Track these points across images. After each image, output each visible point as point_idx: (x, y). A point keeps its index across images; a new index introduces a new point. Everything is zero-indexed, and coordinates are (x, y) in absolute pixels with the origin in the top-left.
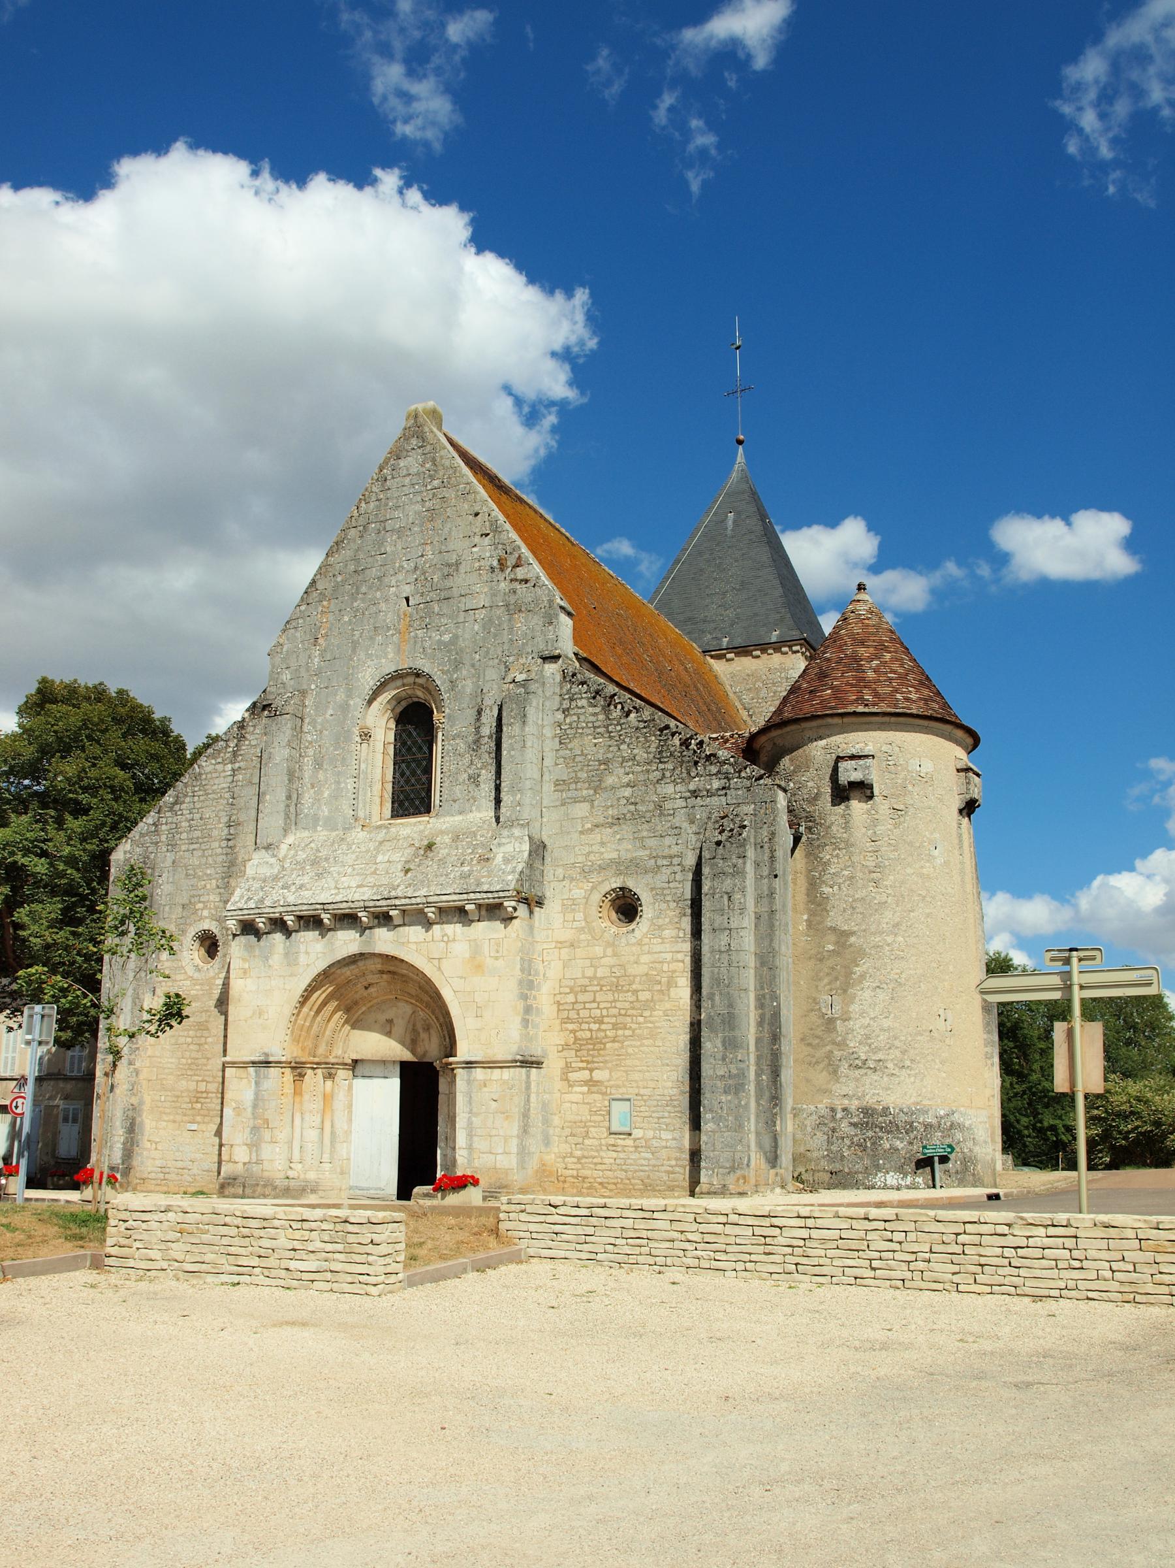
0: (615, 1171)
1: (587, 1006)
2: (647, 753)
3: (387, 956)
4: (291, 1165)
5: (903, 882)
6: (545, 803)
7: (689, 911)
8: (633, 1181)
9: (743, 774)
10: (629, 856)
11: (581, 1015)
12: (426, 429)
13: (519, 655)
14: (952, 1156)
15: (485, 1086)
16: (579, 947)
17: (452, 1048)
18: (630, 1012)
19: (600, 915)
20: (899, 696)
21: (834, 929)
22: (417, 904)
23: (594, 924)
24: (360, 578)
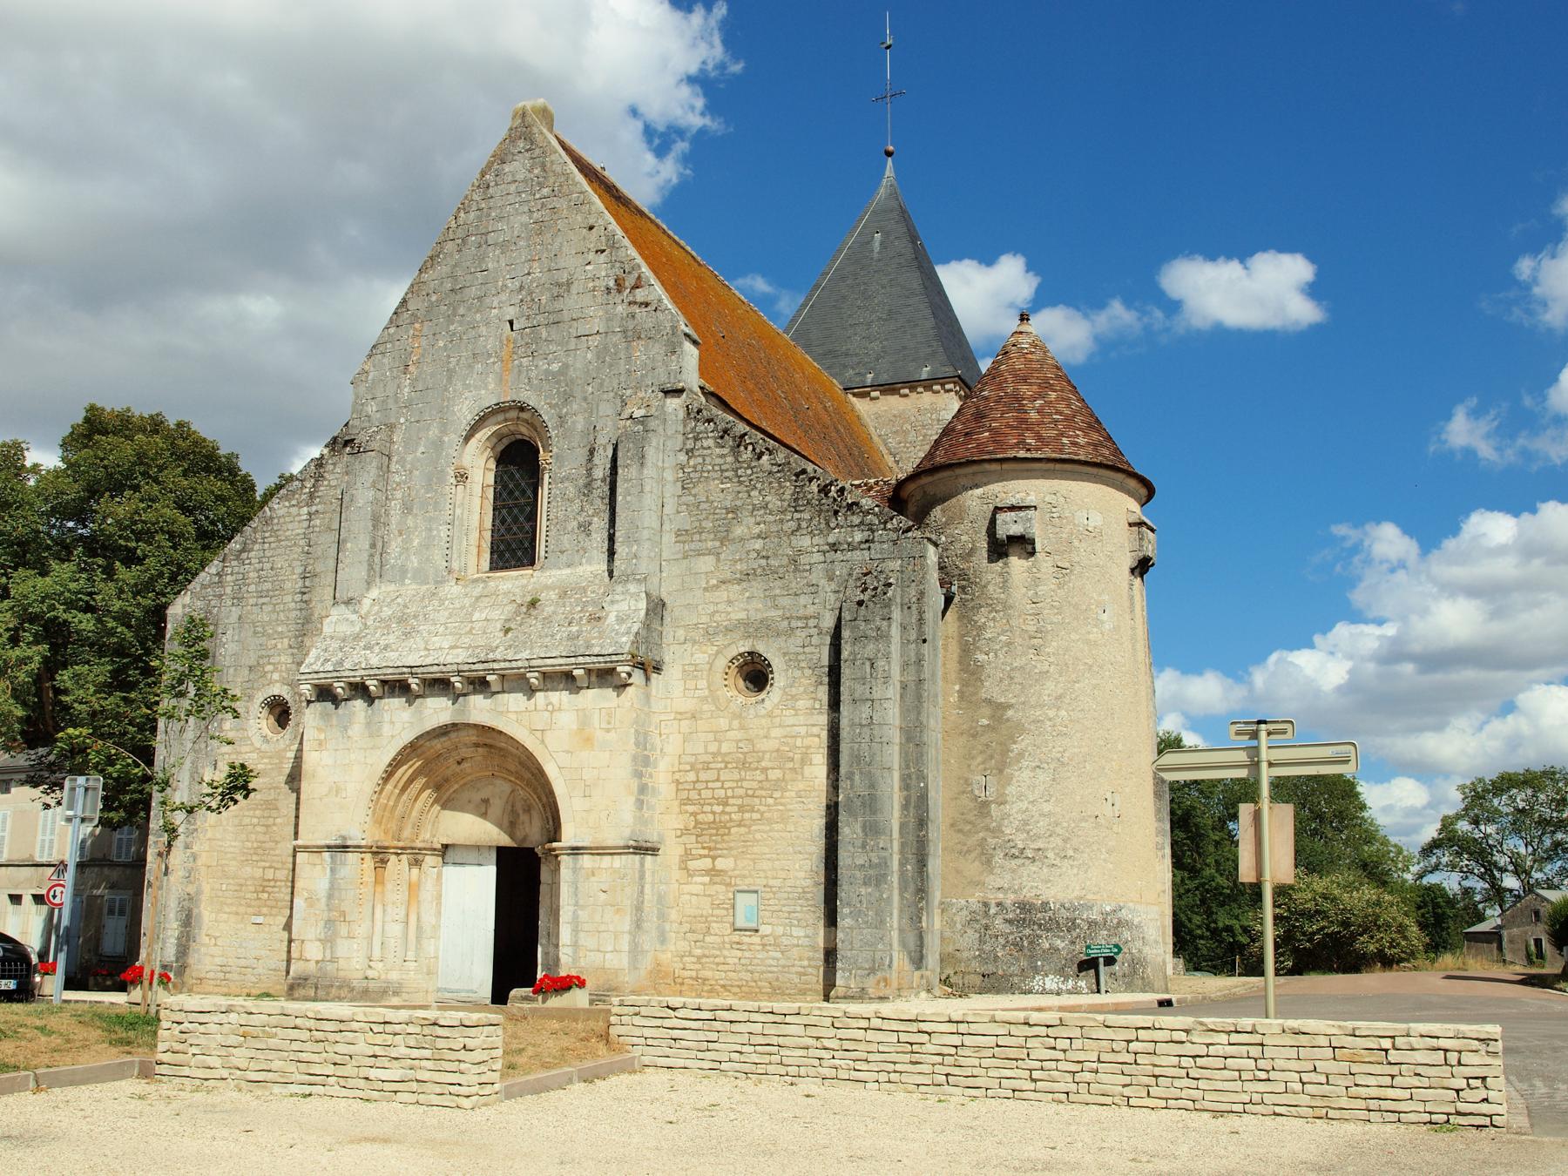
0: (739, 971)
1: (710, 785)
2: (781, 500)
3: (483, 727)
4: (371, 963)
5: (1067, 650)
6: (665, 556)
7: (826, 680)
8: (759, 983)
9: (889, 526)
10: (759, 616)
11: (703, 796)
12: (535, 130)
13: (637, 388)
14: (1119, 958)
15: (593, 875)
16: (702, 719)
17: (555, 833)
18: (758, 793)
19: (726, 683)
20: (1065, 440)
21: (989, 702)
22: (519, 668)
23: (718, 693)
24: (458, 297)
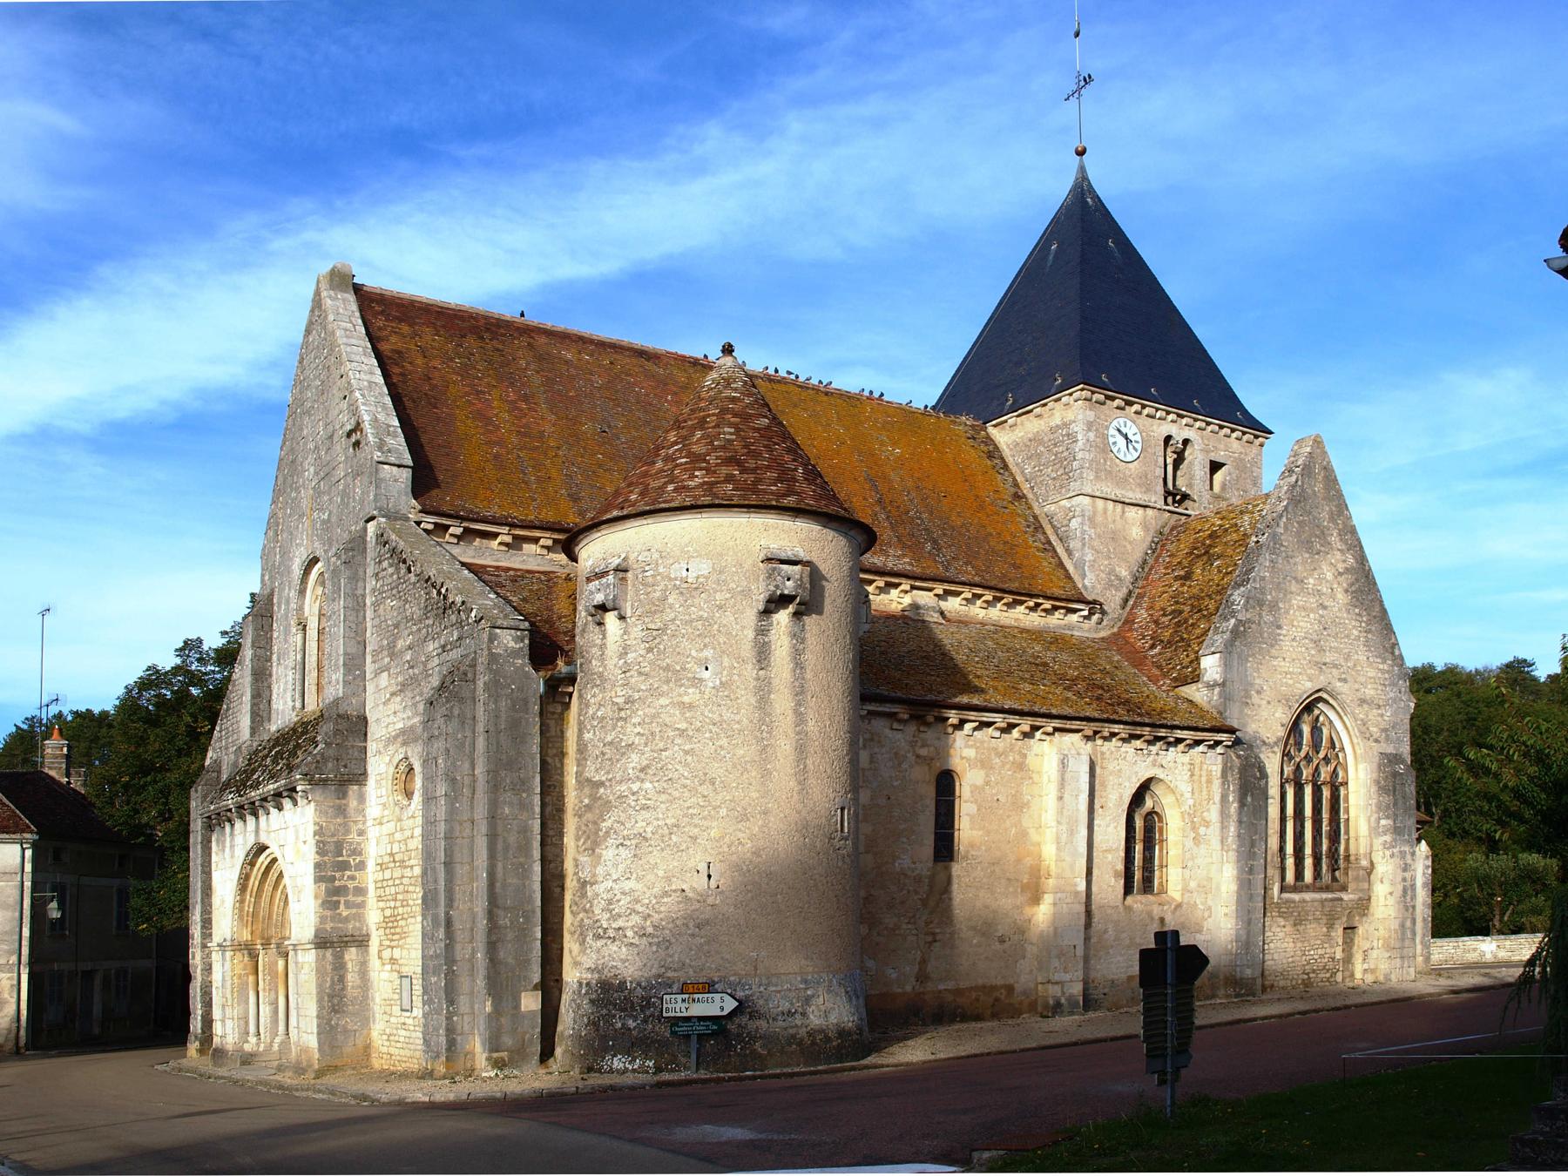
21: (588, 780)
